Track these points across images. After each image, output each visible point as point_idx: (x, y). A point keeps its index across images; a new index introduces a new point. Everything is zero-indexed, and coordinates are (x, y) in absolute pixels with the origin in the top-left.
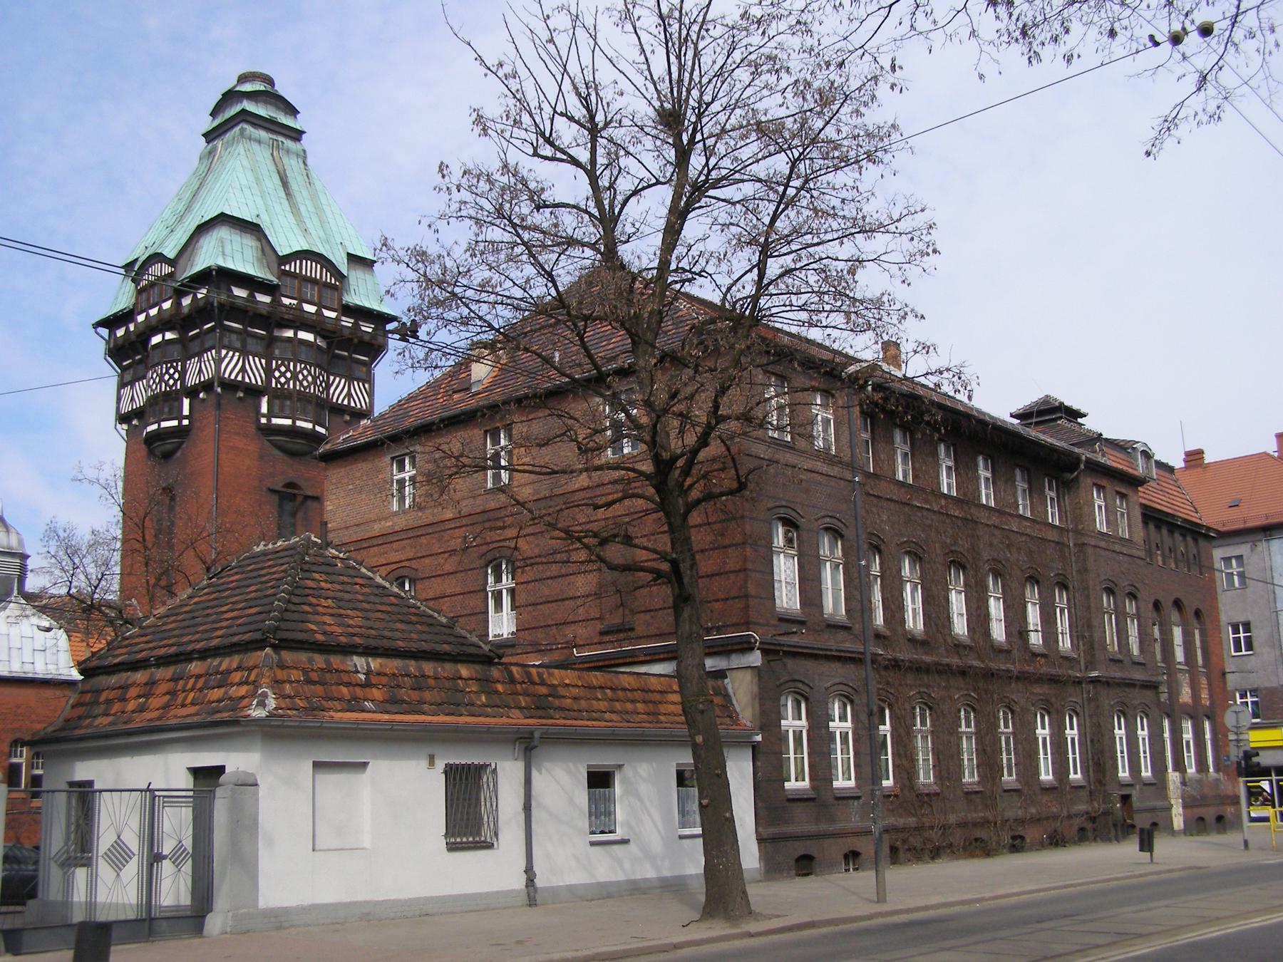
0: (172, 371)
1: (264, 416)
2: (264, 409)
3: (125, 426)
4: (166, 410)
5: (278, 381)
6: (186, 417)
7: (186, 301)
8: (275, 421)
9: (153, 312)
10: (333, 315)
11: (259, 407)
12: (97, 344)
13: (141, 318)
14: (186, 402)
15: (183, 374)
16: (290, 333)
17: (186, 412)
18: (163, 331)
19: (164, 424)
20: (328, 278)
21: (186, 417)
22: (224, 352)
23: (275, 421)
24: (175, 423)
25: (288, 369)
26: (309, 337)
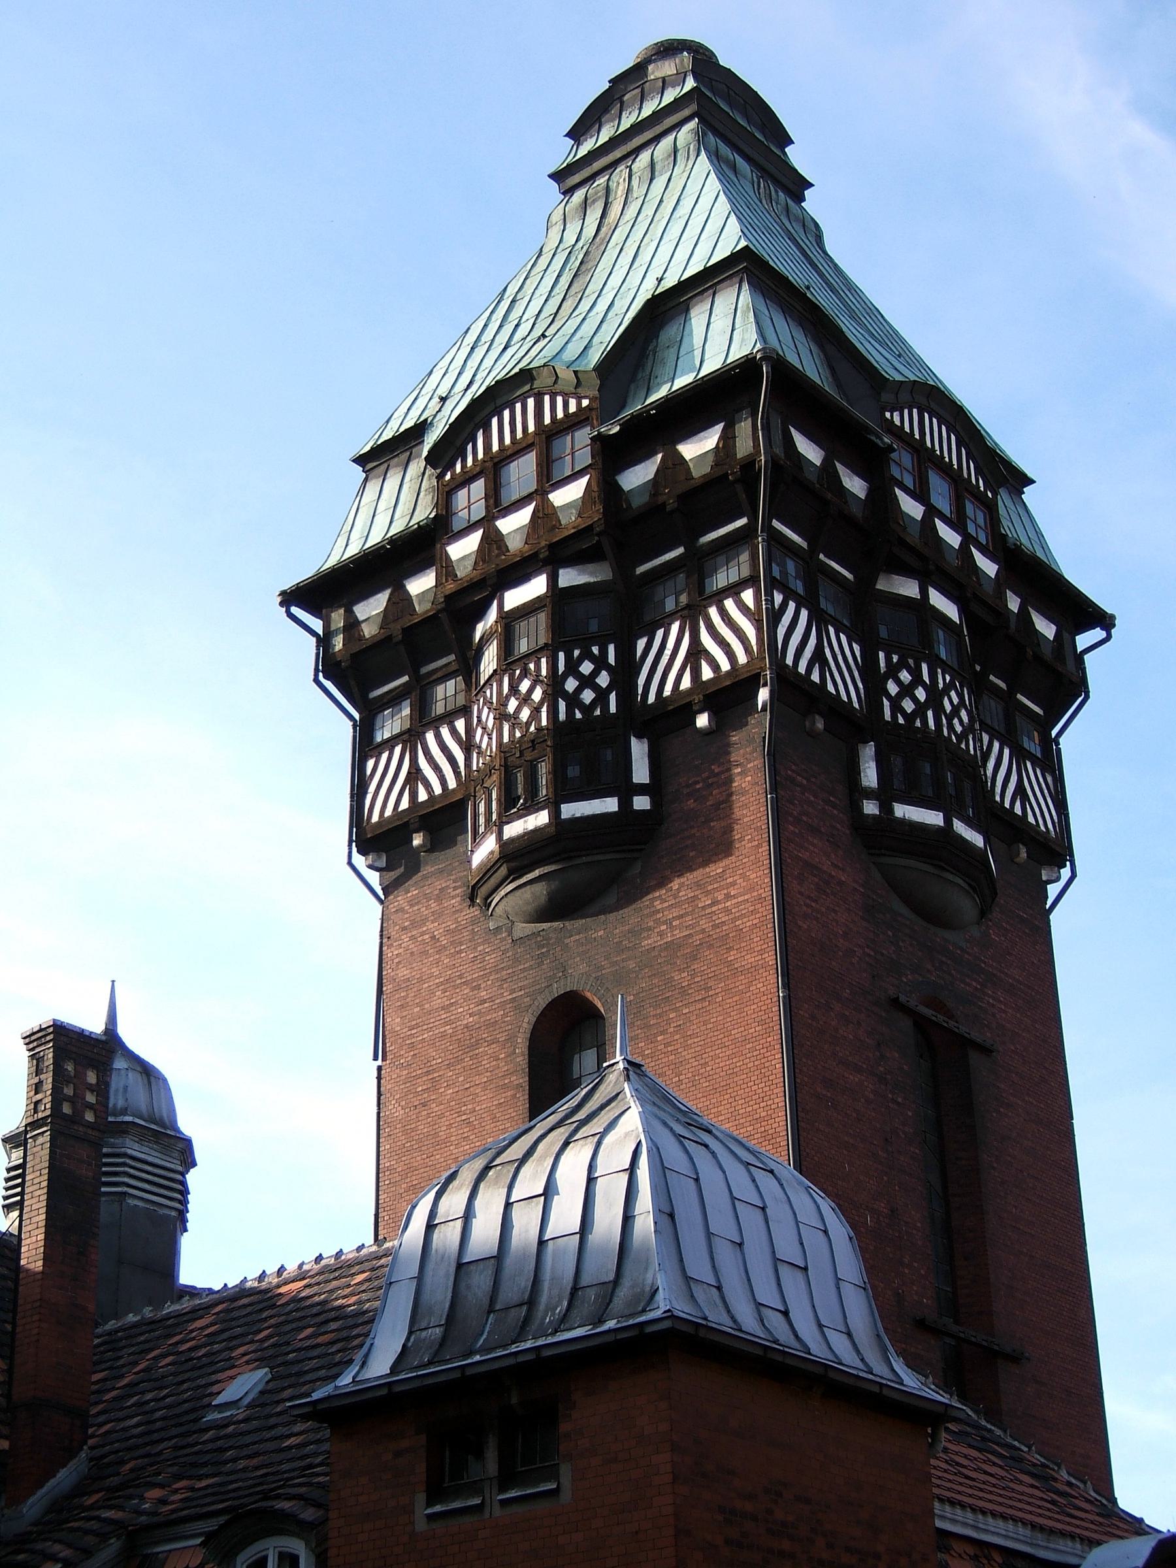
1: (869, 794)
2: (870, 776)
5: (896, 707)
6: (642, 790)
7: (638, 477)
8: (902, 811)
9: (513, 524)
10: (989, 568)
11: (854, 770)
12: (296, 646)
13: (463, 549)
14: (639, 750)
16: (909, 589)
17: (641, 773)
19: (569, 810)
20: (970, 471)
21: (642, 790)
22: (778, 598)
23: (902, 811)
24: (610, 805)
25: (917, 680)
26: (951, 611)
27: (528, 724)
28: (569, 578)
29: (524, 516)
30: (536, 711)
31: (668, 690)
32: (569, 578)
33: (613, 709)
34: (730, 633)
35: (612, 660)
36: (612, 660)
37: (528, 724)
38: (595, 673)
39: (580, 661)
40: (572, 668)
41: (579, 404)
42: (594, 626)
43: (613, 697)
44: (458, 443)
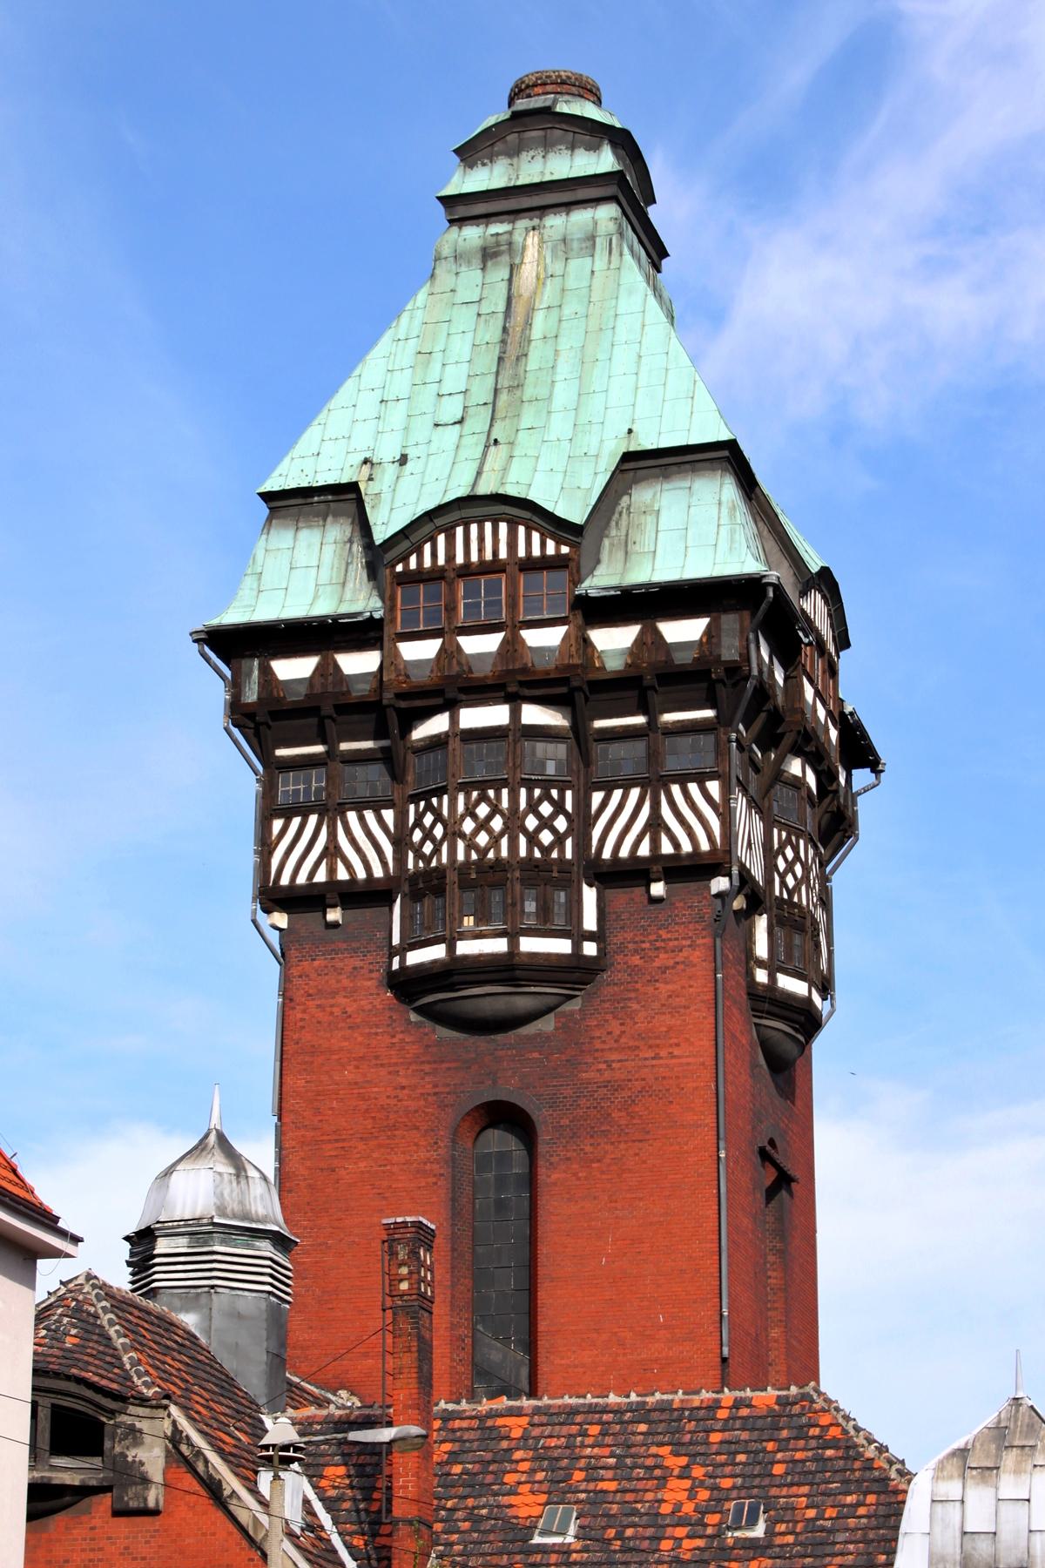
0: (546, 809)
3: (281, 919)
4: (531, 907)
12: (208, 687)
14: (589, 895)
15: (582, 821)
18: (515, 701)
27: (487, 850)
28: (534, 715)
29: (489, 643)
30: (495, 841)
31: (624, 852)
32: (534, 715)
33: (569, 855)
34: (693, 818)
35: (569, 806)
36: (569, 806)
37: (487, 850)
38: (553, 816)
39: (540, 800)
40: (533, 808)
41: (558, 549)
42: (551, 769)
43: (569, 843)
44: (415, 538)
